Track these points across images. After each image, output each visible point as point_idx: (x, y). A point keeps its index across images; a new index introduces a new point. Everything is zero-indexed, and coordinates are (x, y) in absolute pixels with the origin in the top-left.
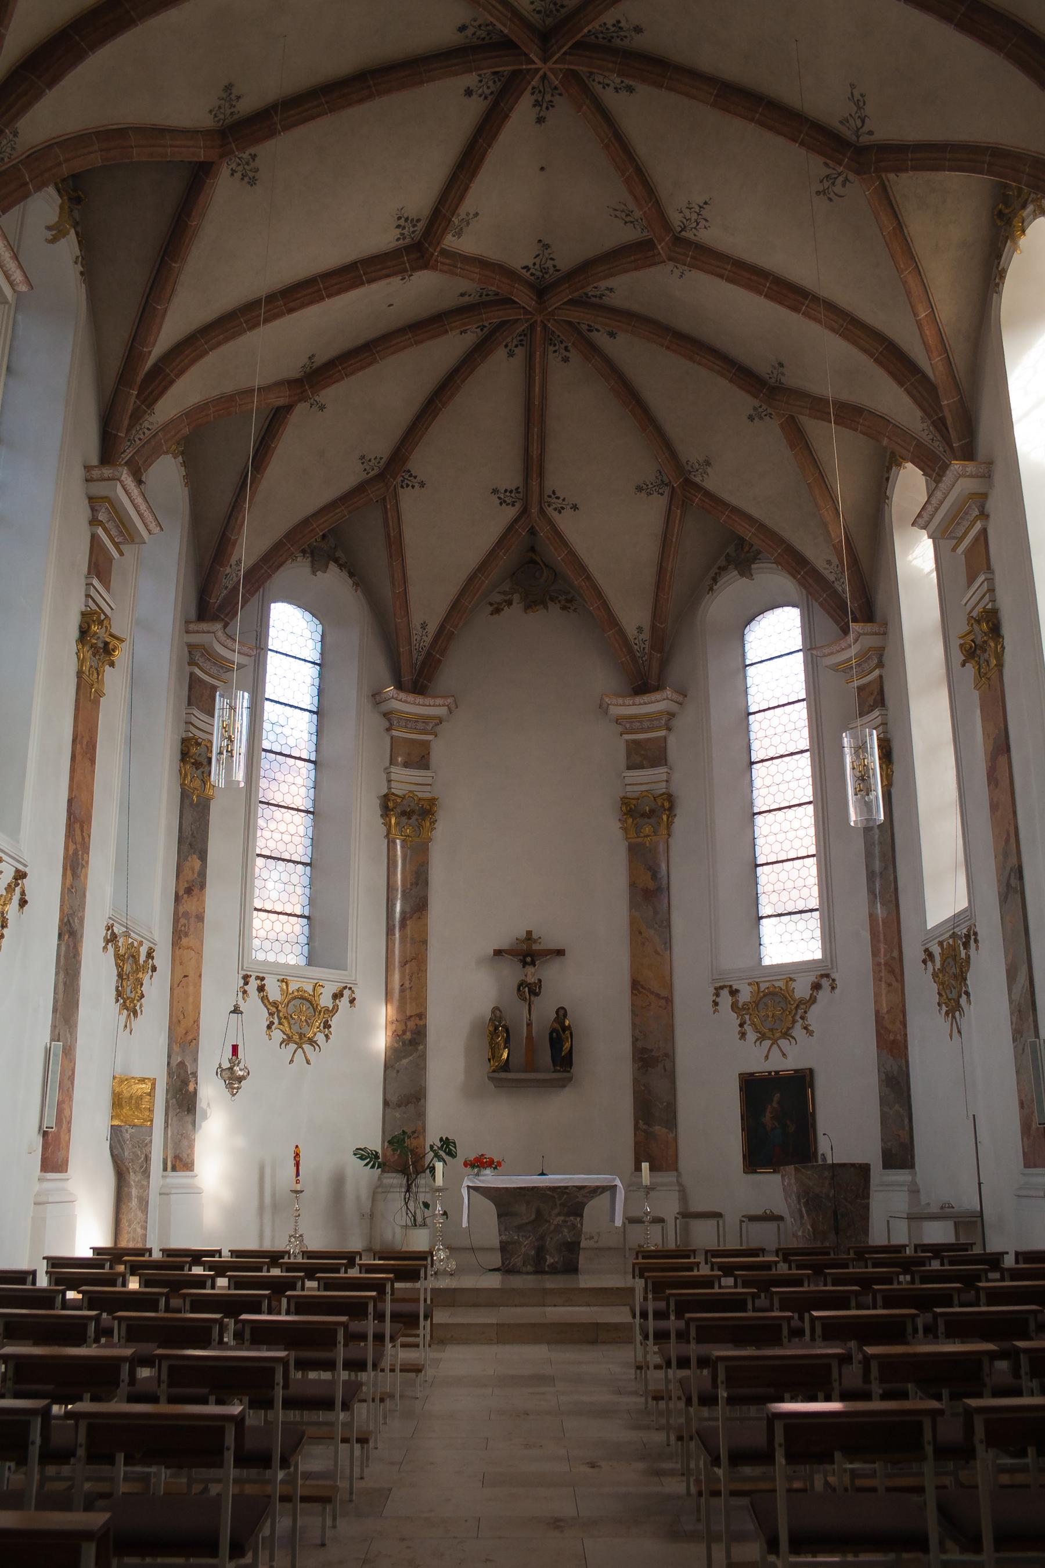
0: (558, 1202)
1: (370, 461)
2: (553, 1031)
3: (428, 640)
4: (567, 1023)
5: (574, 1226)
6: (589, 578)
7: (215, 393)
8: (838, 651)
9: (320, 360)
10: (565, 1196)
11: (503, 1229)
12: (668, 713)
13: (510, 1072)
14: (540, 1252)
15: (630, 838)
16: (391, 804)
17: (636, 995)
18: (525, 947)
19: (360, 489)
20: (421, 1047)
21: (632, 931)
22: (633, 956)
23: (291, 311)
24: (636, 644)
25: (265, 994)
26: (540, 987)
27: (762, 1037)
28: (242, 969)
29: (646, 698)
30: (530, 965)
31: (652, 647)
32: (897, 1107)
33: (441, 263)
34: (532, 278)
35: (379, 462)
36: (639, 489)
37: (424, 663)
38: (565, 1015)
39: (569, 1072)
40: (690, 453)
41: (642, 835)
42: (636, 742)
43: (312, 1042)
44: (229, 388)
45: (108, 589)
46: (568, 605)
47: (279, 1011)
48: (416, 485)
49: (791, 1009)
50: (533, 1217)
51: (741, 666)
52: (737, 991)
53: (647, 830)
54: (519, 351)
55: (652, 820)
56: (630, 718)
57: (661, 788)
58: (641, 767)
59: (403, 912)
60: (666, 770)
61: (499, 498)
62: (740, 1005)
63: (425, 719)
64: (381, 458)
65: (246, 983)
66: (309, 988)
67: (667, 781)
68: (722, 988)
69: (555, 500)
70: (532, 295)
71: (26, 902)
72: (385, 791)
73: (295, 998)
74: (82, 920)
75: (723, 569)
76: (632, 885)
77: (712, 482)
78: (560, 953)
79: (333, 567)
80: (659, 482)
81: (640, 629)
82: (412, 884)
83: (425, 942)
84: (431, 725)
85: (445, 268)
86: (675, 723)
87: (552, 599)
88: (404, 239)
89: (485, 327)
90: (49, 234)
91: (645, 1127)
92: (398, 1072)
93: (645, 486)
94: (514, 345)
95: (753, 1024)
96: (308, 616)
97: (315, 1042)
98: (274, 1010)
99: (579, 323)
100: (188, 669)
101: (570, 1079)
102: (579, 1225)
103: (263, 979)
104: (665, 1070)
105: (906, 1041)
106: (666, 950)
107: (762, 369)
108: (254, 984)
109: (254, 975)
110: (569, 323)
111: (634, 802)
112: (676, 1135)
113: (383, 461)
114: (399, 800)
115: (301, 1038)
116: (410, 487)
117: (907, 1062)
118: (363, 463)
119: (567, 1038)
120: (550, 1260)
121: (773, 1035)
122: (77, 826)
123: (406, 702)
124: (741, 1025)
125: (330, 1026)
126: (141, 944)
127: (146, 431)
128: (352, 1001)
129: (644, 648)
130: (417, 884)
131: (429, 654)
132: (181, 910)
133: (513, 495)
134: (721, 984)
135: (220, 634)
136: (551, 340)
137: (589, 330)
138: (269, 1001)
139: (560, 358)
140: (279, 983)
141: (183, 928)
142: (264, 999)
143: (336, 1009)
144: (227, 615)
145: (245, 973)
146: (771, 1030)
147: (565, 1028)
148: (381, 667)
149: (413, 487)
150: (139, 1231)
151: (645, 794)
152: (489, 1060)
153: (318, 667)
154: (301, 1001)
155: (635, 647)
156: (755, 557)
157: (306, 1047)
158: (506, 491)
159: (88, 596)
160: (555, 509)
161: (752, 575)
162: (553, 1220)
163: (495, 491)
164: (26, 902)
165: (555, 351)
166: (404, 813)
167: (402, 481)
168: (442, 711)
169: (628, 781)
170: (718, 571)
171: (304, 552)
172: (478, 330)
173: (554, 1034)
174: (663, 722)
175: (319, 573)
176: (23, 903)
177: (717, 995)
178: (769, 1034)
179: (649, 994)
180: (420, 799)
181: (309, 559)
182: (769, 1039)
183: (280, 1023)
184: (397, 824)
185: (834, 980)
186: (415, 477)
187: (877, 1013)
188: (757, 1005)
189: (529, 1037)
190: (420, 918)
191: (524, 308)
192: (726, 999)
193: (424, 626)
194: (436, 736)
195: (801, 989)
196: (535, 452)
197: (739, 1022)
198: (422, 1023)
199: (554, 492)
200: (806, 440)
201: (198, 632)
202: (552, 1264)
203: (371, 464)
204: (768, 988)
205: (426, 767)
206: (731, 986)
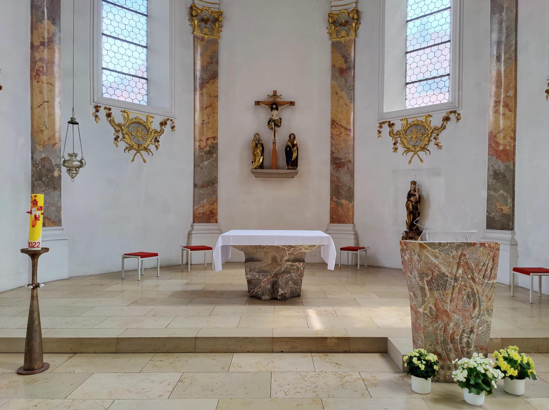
0: (287, 253)
2: (288, 146)
4: (295, 143)
5: (298, 269)
10: (293, 249)
11: (248, 270)
13: (264, 169)
14: (275, 285)
15: (333, 38)
16: (194, 13)
17: (334, 128)
18: (271, 100)
20: (215, 155)
21: (332, 93)
25: (112, 119)
26: (280, 122)
28: (94, 101)
30: (275, 110)
32: (501, 192)
38: (294, 138)
39: (296, 169)
41: (340, 36)
43: (146, 149)
47: (122, 130)
52: (393, 124)
53: (343, 33)
55: (346, 28)
59: (202, 78)
62: (395, 132)
65: (97, 111)
68: (384, 123)
73: (133, 123)
76: (333, 66)
78: (292, 103)
83: (217, 97)
91: (336, 200)
92: (202, 168)
95: (402, 142)
97: (149, 150)
98: (119, 128)
101: (297, 173)
102: (302, 268)
103: (110, 109)
104: (348, 170)
105: (514, 150)
106: (351, 103)
108: (102, 113)
111: (336, 17)
112: (353, 204)
114: (199, 11)
115: (139, 147)
117: (514, 163)
119: (295, 150)
120: (281, 292)
124: (395, 144)
125: (158, 141)
128: (173, 127)
130: (211, 63)
134: (384, 121)
138: (115, 123)
140: (122, 113)
141: (41, 69)
142: (112, 122)
143: (162, 132)
147: (294, 145)
151: (342, 11)
152: (252, 162)
154: (137, 125)
162: (284, 264)
166: (203, 20)
173: (288, 148)
178: (412, 149)
179: (341, 128)
183: (124, 138)
184: (199, 26)
188: (406, 132)
189: (274, 150)
190: (213, 83)
192: (386, 129)
195: (436, 121)
197: (393, 142)
198: (215, 142)
202: (282, 294)
206: (389, 122)
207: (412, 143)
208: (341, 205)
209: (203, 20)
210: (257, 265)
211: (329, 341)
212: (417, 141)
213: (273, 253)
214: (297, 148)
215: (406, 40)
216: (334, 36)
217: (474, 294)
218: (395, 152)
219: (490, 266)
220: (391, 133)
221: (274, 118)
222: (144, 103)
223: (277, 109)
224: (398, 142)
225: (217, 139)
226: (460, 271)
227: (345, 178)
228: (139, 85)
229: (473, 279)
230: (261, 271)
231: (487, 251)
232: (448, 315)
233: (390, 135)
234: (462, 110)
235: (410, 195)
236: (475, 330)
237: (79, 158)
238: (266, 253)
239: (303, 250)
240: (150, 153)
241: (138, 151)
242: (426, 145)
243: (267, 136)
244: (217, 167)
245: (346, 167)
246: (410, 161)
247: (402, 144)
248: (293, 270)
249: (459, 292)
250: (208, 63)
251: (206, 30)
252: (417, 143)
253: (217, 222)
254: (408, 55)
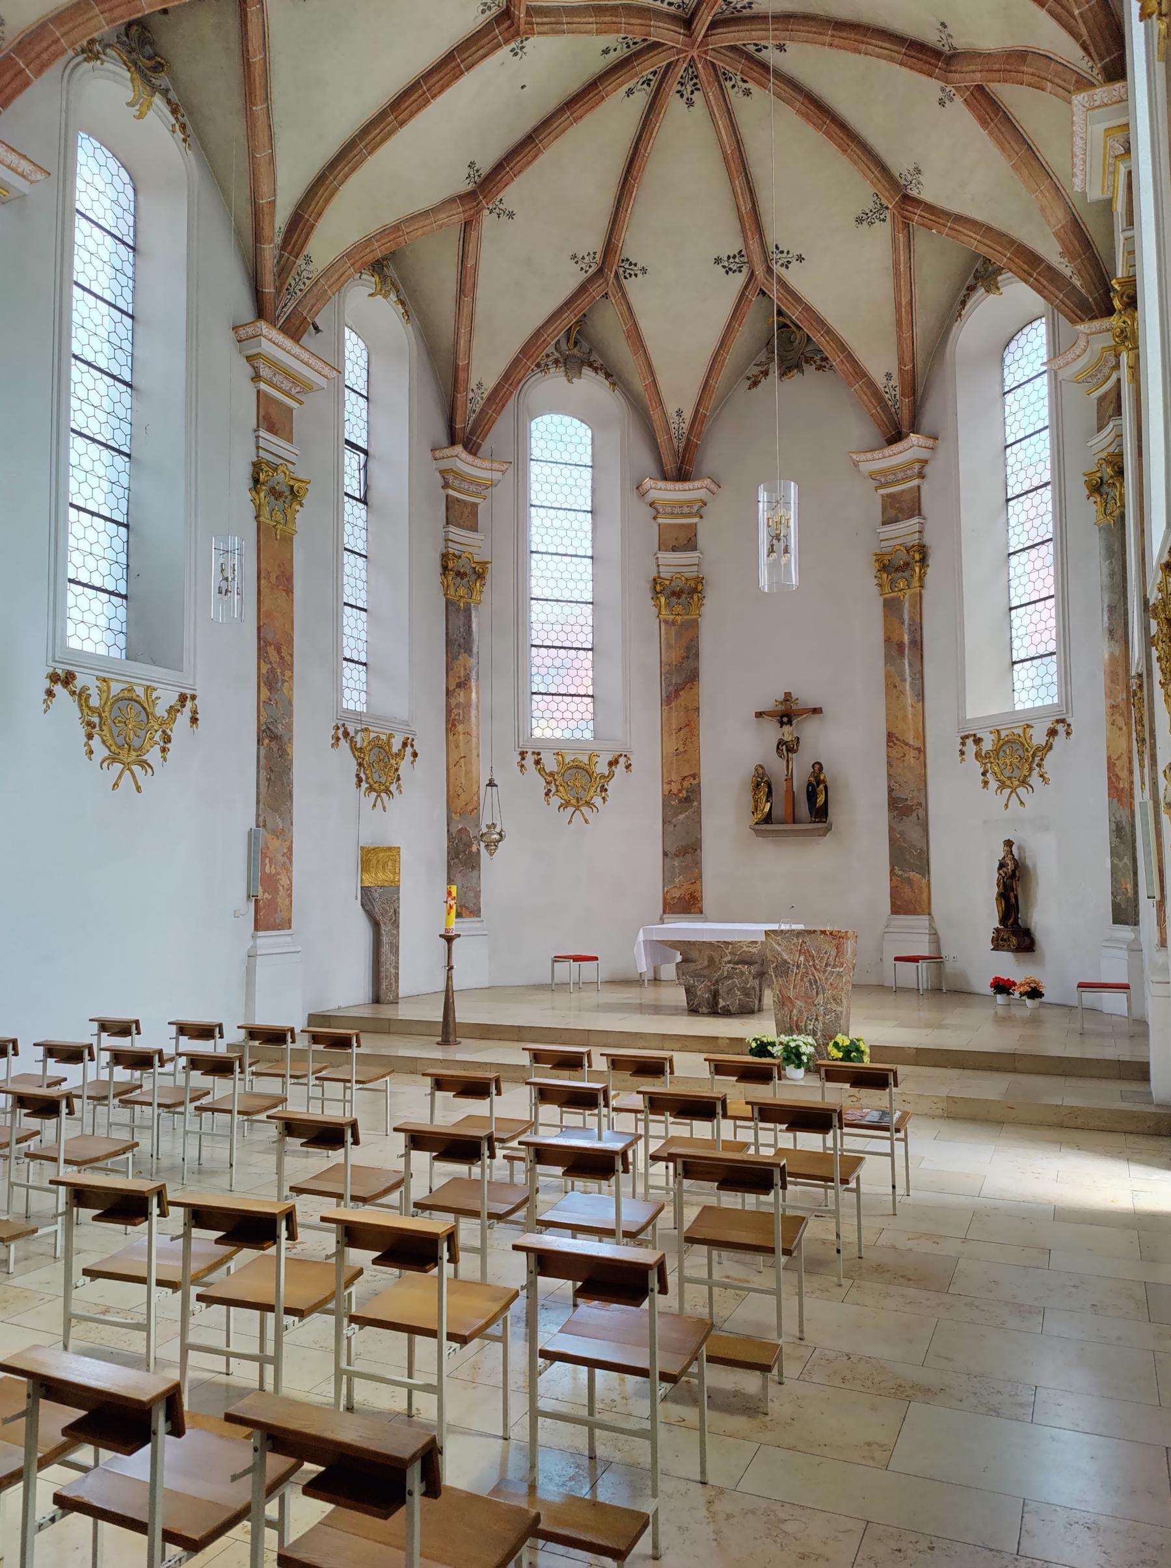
0: (727, 951)
1: (583, 258)
2: (810, 784)
3: (685, 426)
4: (822, 778)
6: (829, 332)
7: (374, 227)
8: (1074, 360)
9: (485, 166)
11: (680, 973)
12: (919, 461)
16: (658, 588)
18: (781, 708)
19: (582, 289)
20: (695, 804)
21: (887, 685)
22: (888, 709)
23: (402, 124)
24: (887, 393)
26: (798, 742)
27: (1002, 786)
29: (895, 448)
31: (903, 394)
33: (537, 24)
34: (673, 8)
35: (594, 258)
36: (860, 220)
37: (685, 449)
39: (825, 822)
40: (899, 165)
42: (891, 496)
43: (588, 804)
44: (390, 219)
45: (290, 440)
46: (824, 364)
47: (555, 780)
48: (638, 272)
50: (706, 963)
51: (998, 392)
54: (697, 97)
55: (906, 574)
56: (883, 472)
57: (914, 540)
58: (895, 520)
60: (917, 521)
61: (724, 267)
63: (690, 503)
64: (595, 253)
65: (523, 759)
66: (585, 760)
67: (920, 532)
68: (967, 737)
69: (780, 255)
70: (677, 29)
71: (197, 719)
72: (656, 575)
73: (570, 768)
74: (289, 727)
75: (971, 289)
76: (888, 640)
77: (928, 192)
78: (816, 711)
79: (587, 371)
80: (878, 207)
81: (889, 376)
82: (683, 658)
83: (697, 710)
84: (696, 508)
85: (546, 28)
86: (928, 470)
87: (807, 362)
88: (490, 8)
89: (650, 80)
90: (134, 110)
91: (900, 873)
92: (675, 826)
93: (865, 216)
94: (689, 92)
96: (576, 422)
99: (744, 45)
100: (443, 493)
103: (539, 754)
106: (919, 702)
107: (931, 37)
108: (530, 759)
109: (530, 751)
110: (733, 48)
113: (598, 256)
114: (667, 582)
116: (633, 276)
118: (577, 262)
122: (271, 650)
123: (666, 490)
124: (984, 774)
125: (606, 790)
126: (391, 736)
127: (305, 280)
128: (628, 767)
129: (895, 395)
130: (688, 657)
131: (688, 439)
132: (453, 702)
133: (737, 260)
134: (966, 733)
135: (464, 455)
136: (724, 74)
137: (757, 50)
139: (741, 93)
140: (555, 756)
141: (457, 717)
142: (541, 771)
143: (611, 775)
144: (478, 438)
145: (520, 750)
146: (1010, 778)
147: (819, 782)
148: (645, 460)
149: (636, 275)
150: (393, 971)
151: (897, 548)
153: (590, 469)
154: (576, 770)
155: (887, 396)
156: (999, 271)
157: (584, 809)
158: (729, 257)
159: (258, 447)
160: (782, 265)
161: (998, 289)
163: (718, 261)
164: (197, 719)
165: (733, 86)
166: (674, 594)
167: (624, 272)
168: (701, 494)
169: (882, 537)
170: (966, 292)
171: (556, 362)
172: (645, 86)
174: (916, 470)
175: (574, 380)
176: (194, 720)
177: (963, 744)
178: (1008, 783)
180: (687, 580)
181: (563, 368)
182: (1009, 787)
183: (557, 791)
184: (667, 604)
185: (1069, 725)
186: (635, 265)
187: (1109, 758)
188: (998, 754)
191: (673, 47)
192: (971, 747)
193: (679, 413)
194: (701, 517)
195: (1038, 737)
196: (743, 208)
197: (982, 770)
198: (696, 782)
199: (777, 247)
200: (1004, 112)
201: (443, 458)
202: (724, 1007)
203: (585, 261)
205: (694, 548)
206: (975, 735)
207: (1007, 773)
208: (909, 881)
209: (674, 594)
210: (691, 967)
211: (720, 1041)
213: (708, 952)
214: (826, 788)
215: (1009, 587)
216: (887, 589)
217: (816, 982)
219: (834, 952)
221: (786, 739)
222: (588, 735)
223: (790, 723)
225: (699, 777)
226: (802, 958)
227: (914, 835)
228: (582, 708)
229: (814, 966)
230: (697, 975)
231: (830, 938)
232: (792, 1002)
235: (1002, 865)
236: (820, 1018)
237: (498, 830)
238: (700, 951)
239: (745, 949)
240: (595, 809)
241: (577, 808)
242: (1026, 777)
243: (776, 767)
244: (700, 822)
245: (914, 814)
248: (736, 974)
249: (802, 980)
250: (683, 658)
251: (679, 609)
253: (702, 913)
254: (1013, 612)
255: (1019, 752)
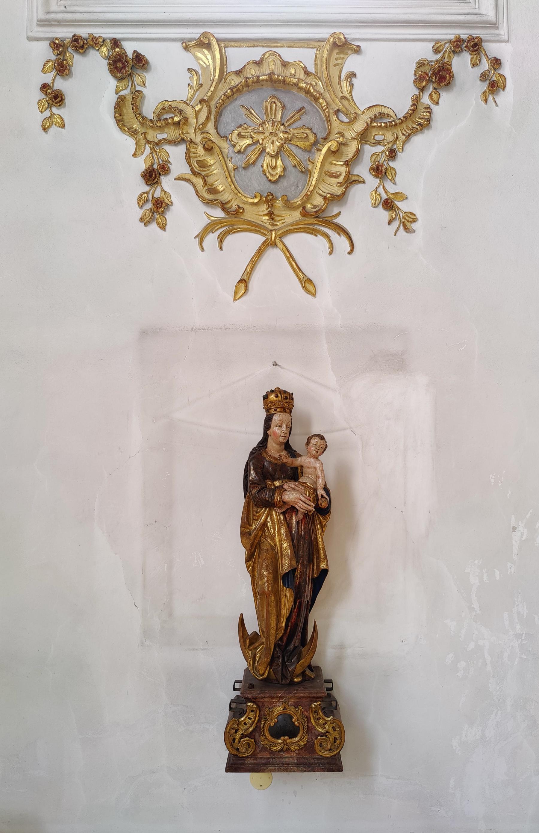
49: (341, 134)
121: (271, 214)
134: (83, 32)
204: (259, 63)
206: (116, 43)
212: (284, 169)
218: (154, 226)
220: (128, 110)
224: (172, 167)
233: (120, 121)
234: (509, 45)
246: (244, 282)
247: (199, 182)
252: (284, 183)
255: (306, 120)
